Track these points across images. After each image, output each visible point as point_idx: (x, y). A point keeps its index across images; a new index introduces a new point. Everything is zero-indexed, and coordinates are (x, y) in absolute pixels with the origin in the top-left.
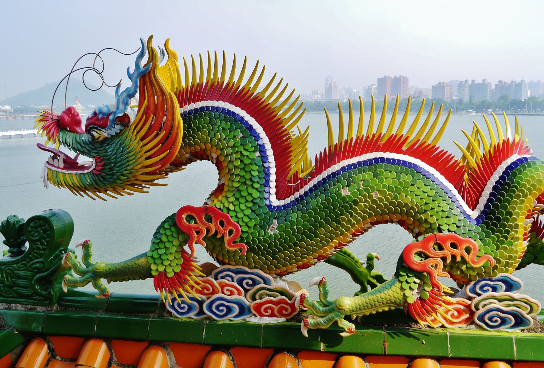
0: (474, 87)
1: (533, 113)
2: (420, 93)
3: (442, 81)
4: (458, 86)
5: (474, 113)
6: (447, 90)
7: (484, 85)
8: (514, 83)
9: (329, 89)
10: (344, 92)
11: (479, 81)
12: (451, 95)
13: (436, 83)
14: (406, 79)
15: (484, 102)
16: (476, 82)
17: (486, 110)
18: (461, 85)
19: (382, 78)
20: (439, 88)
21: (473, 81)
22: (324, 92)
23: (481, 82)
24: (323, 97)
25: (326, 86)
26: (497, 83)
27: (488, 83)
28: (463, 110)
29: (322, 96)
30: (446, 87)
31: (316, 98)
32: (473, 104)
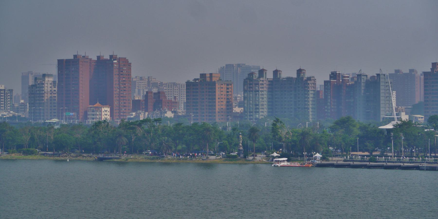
1: (406, 161)
3: (207, 72)
5: (284, 162)
6: (220, 92)
11: (289, 72)
12: (229, 106)
15: (304, 135)
16: (284, 75)
20: (200, 88)
21: (276, 72)
26: (328, 79)
27: (309, 79)
28: (259, 150)
30: (217, 86)
32: (280, 139)
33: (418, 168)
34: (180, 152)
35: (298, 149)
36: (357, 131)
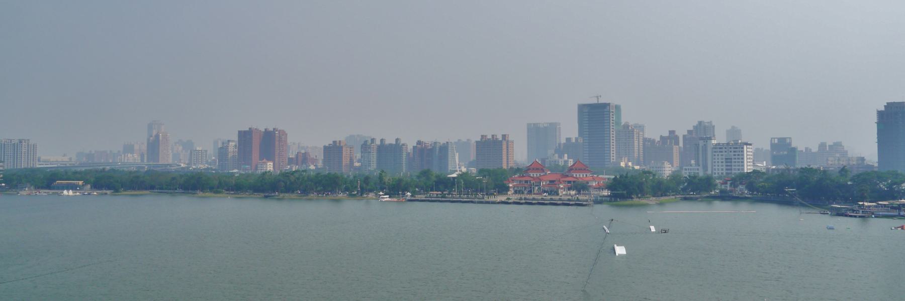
0: (383, 149)
2: (304, 158)
3: (338, 140)
5: (386, 198)
7: (397, 148)
9: (154, 146)
10: (181, 148)
11: (390, 140)
13: (328, 142)
14: (283, 133)
15: (400, 181)
16: (387, 142)
19: (245, 132)
20: (333, 151)
21: (382, 140)
22: (144, 148)
24: (142, 160)
25: (148, 140)
28: (371, 191)
29: (142, 156)
30: (344, 149)
31: (131, 161)
32: (384, 183)
33: (472, 202)
34: (319, 192)
35: (396, 189)
36: (434, 178)
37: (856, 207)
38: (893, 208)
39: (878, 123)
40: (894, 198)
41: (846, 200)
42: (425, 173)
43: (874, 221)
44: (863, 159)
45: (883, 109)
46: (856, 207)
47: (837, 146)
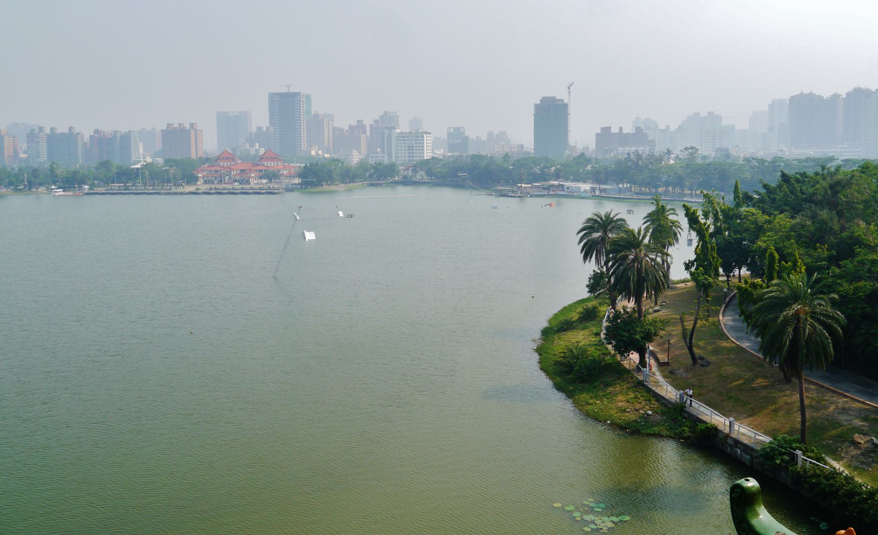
0: (54, 139)
4: (28, 136)
5: (60, 192)
7: (71, 137)
8: (119, 135)
11: (62, 129)
12: (16, 153)
15: (75, 173)
16: (59, 131)
17: (80, 188)
18: (32, 136)
21: (52, 129)
23: (67, 131)
26: (92, 134)
27: (78, 134)
28: (41, 185)
30: (5, 138)
32: (57, 176)
33: (158, 193)
36: (114, 170)
37: (515, 189)
38: (544, 188)
39: (535, 115)
40: (545, 180)
41: (507, 183)
42: (105, 164)
43: (529, 201)
44: (522, 146)
45: (539, 102)
46: (515, 189)
47: (502, 134)
